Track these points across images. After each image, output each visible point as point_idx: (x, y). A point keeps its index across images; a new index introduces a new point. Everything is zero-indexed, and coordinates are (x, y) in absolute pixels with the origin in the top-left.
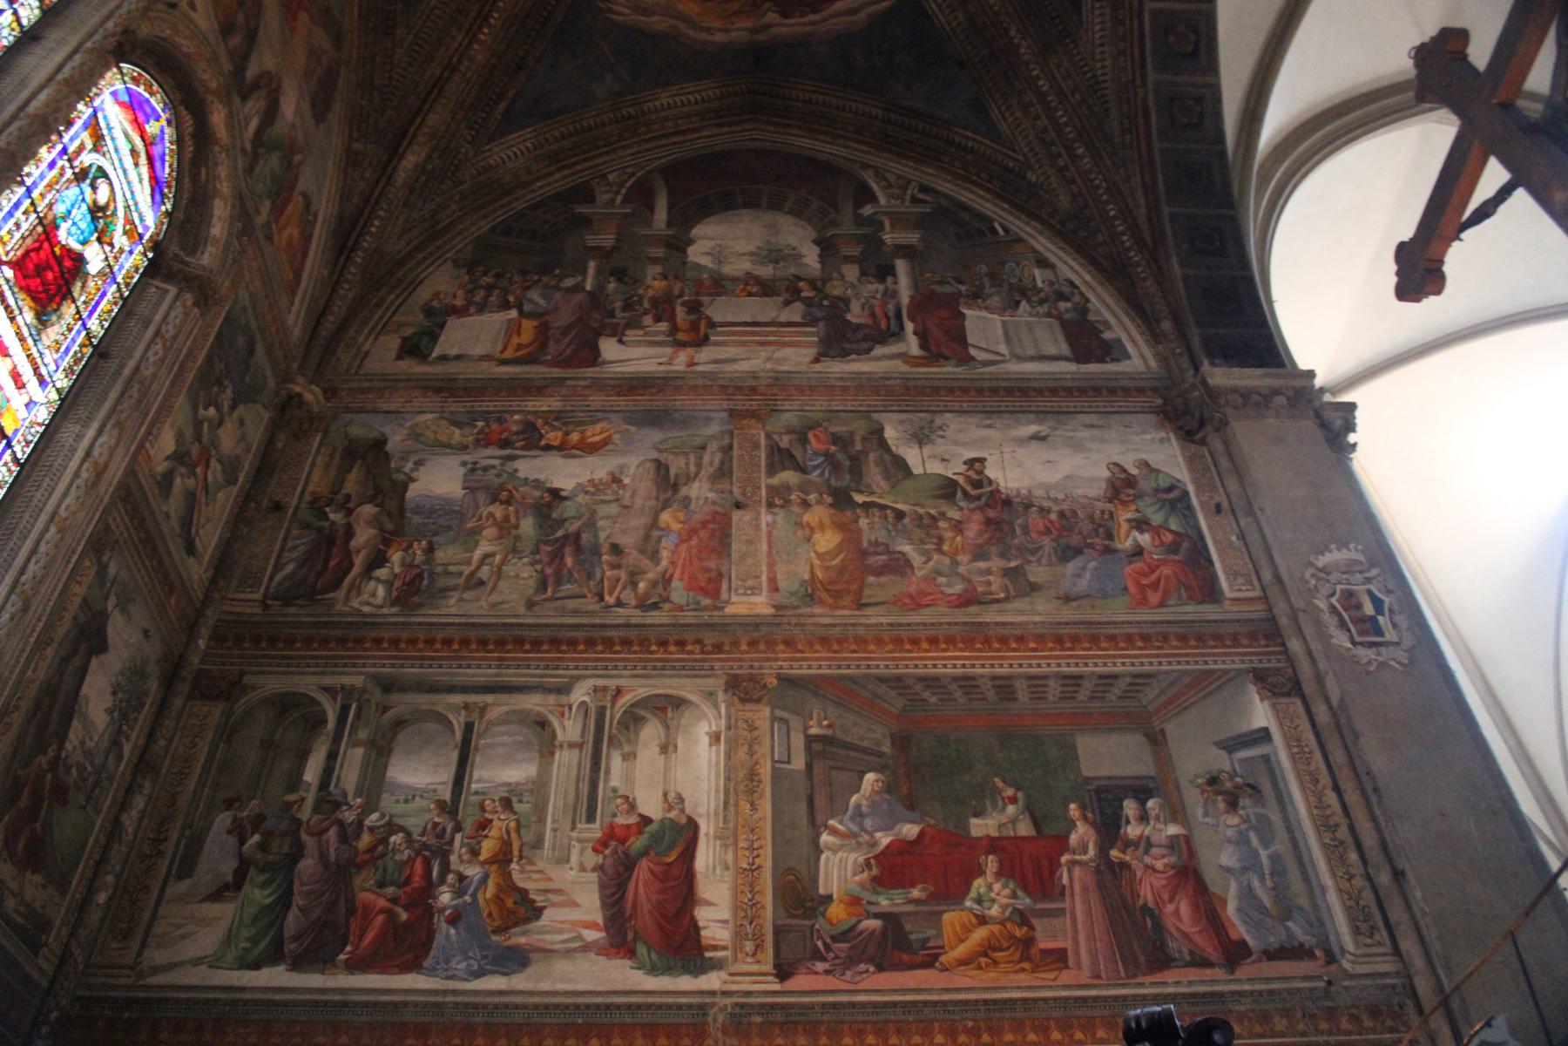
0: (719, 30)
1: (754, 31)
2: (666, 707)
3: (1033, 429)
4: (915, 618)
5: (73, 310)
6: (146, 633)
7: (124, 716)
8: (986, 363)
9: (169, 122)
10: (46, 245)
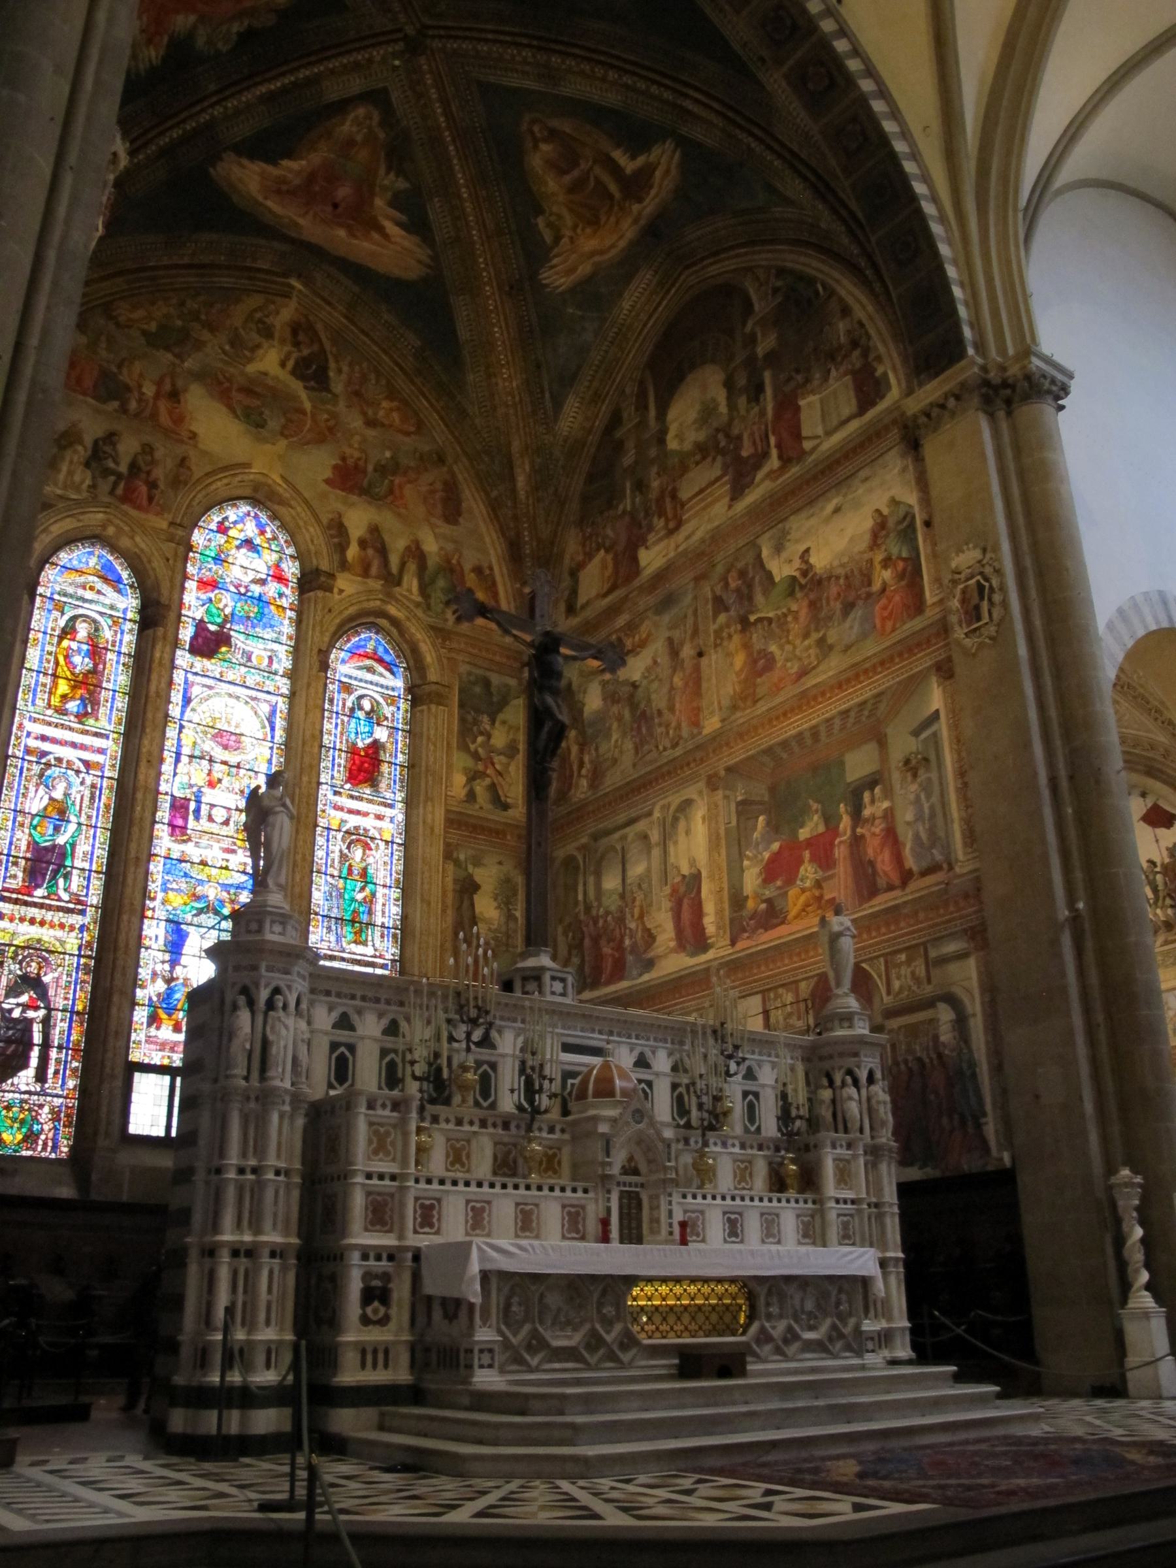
0: (617, 241)
1: (636, 221)
2: (687, 804)
3: (830, 507)
4: (779, 699)
5: (386, 765)
6: (500, 863)
7: (507, 903)
8: (814, 449)
9: (377, 633)
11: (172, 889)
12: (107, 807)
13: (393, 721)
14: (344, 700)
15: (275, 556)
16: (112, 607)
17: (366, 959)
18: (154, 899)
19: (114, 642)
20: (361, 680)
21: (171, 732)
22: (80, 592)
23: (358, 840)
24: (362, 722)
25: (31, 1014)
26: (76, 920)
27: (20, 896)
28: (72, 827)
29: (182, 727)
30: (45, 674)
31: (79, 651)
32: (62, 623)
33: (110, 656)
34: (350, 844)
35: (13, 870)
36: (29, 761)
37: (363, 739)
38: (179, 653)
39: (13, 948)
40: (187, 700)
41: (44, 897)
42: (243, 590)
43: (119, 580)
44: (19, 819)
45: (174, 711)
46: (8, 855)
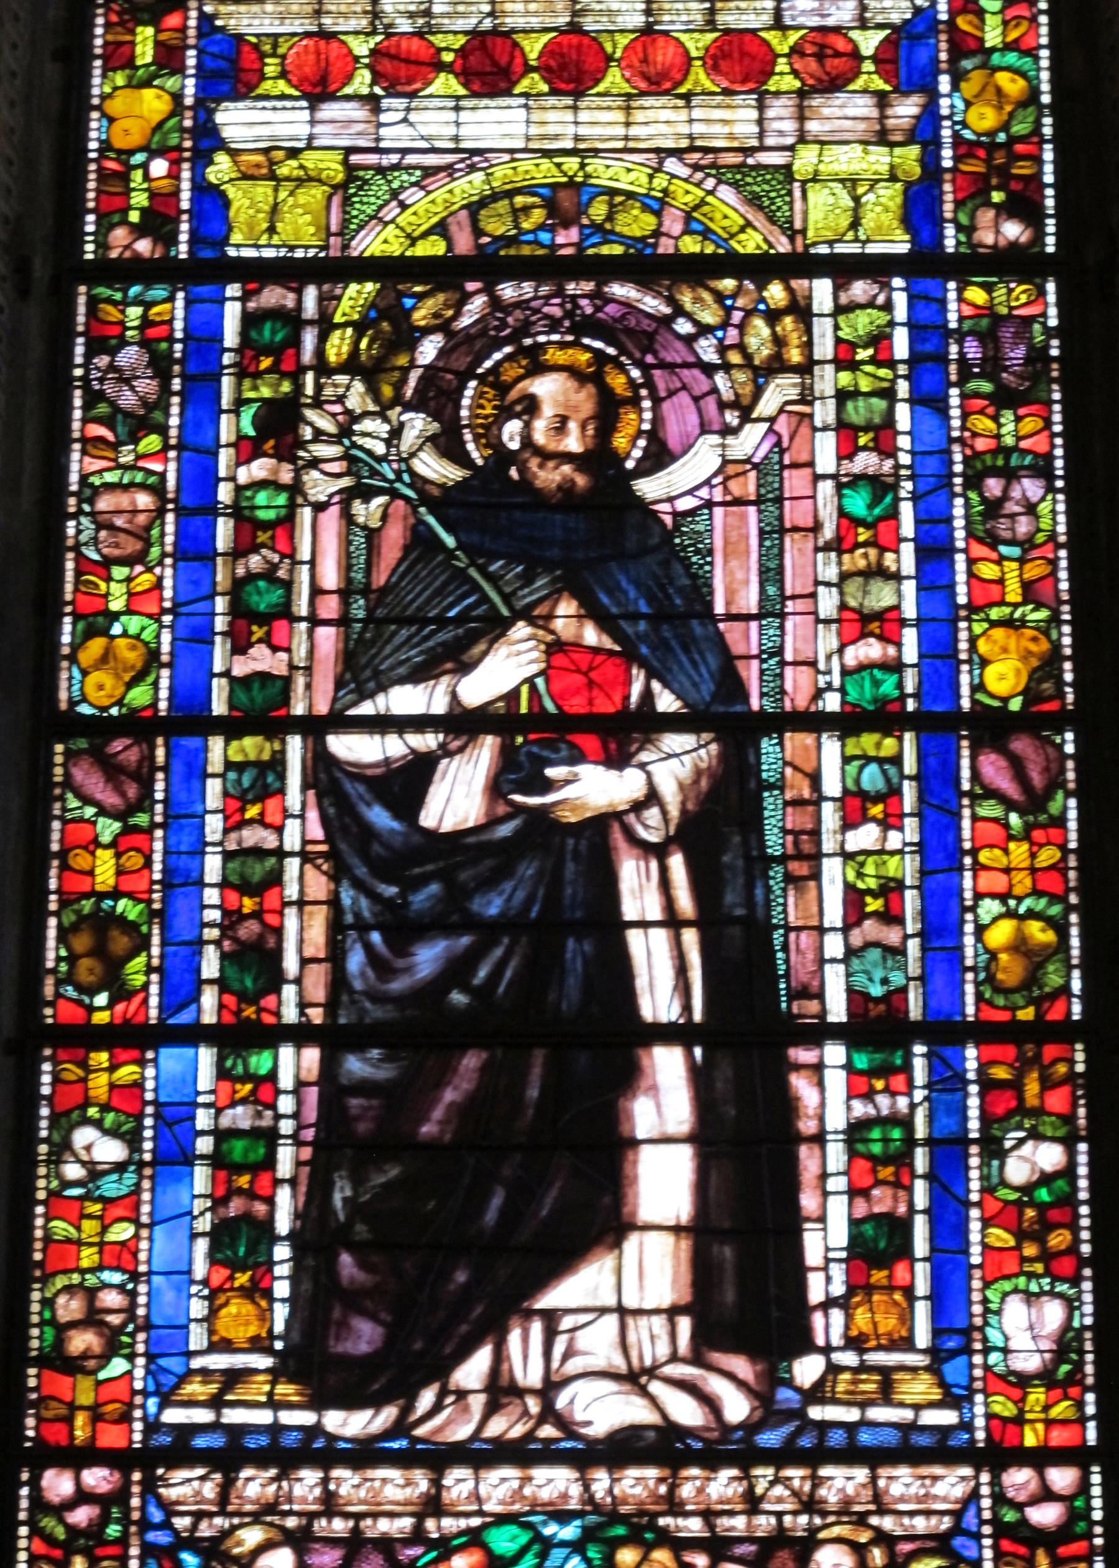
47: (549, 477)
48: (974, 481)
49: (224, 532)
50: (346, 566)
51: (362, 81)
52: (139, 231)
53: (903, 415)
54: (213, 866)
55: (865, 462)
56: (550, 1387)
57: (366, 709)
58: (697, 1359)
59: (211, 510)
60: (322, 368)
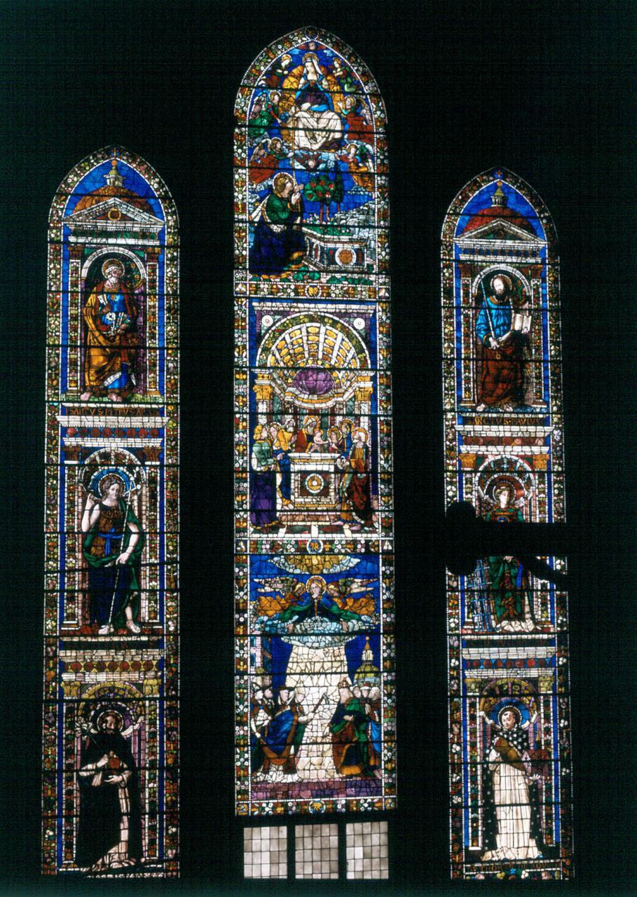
10: (490, 363)
11: (265, 594)
12: (172, 504)
13: (537, 299)
14: (466, 286)
15: (350, 101)
16: (144, 235)
17: (525, 637)
18: (245, 611)
19: (153, 281)
20: (487, 253)
21: (240, 389)
22: (101, 224)
23: (501, 479)
24: (494, 312)
25: (115, 779)
26: (155, 655)
27: (82, 639)
28: (134, 539)
29: (254, 377)
30: (74, 347)
31: (111, 304)
32: (84, 273)
33: (150, 303)
34: (491, 486)
35: (70, 607)
36: (70, 466)
37: (497, 336)
38: (238, 275)
39: (82, 704)
40: (256, 338)
41: (110, 635)
42: (311, 163)
43: (148, 193)
44: (69, 542)
45: (242, 358)
46: (62, 590)
47: (110, 732)
48: (167, 732)
49: (64, 741)
50: (81, 747)
51: (82, 670)
52: (51, 694)
53: (158, 722)
54: (64, 791)
55: (152, 729)
56: (110, 863)
57: (84, 768)
58: (129, 859)
59: (62, 738)
60: (77, 716)
